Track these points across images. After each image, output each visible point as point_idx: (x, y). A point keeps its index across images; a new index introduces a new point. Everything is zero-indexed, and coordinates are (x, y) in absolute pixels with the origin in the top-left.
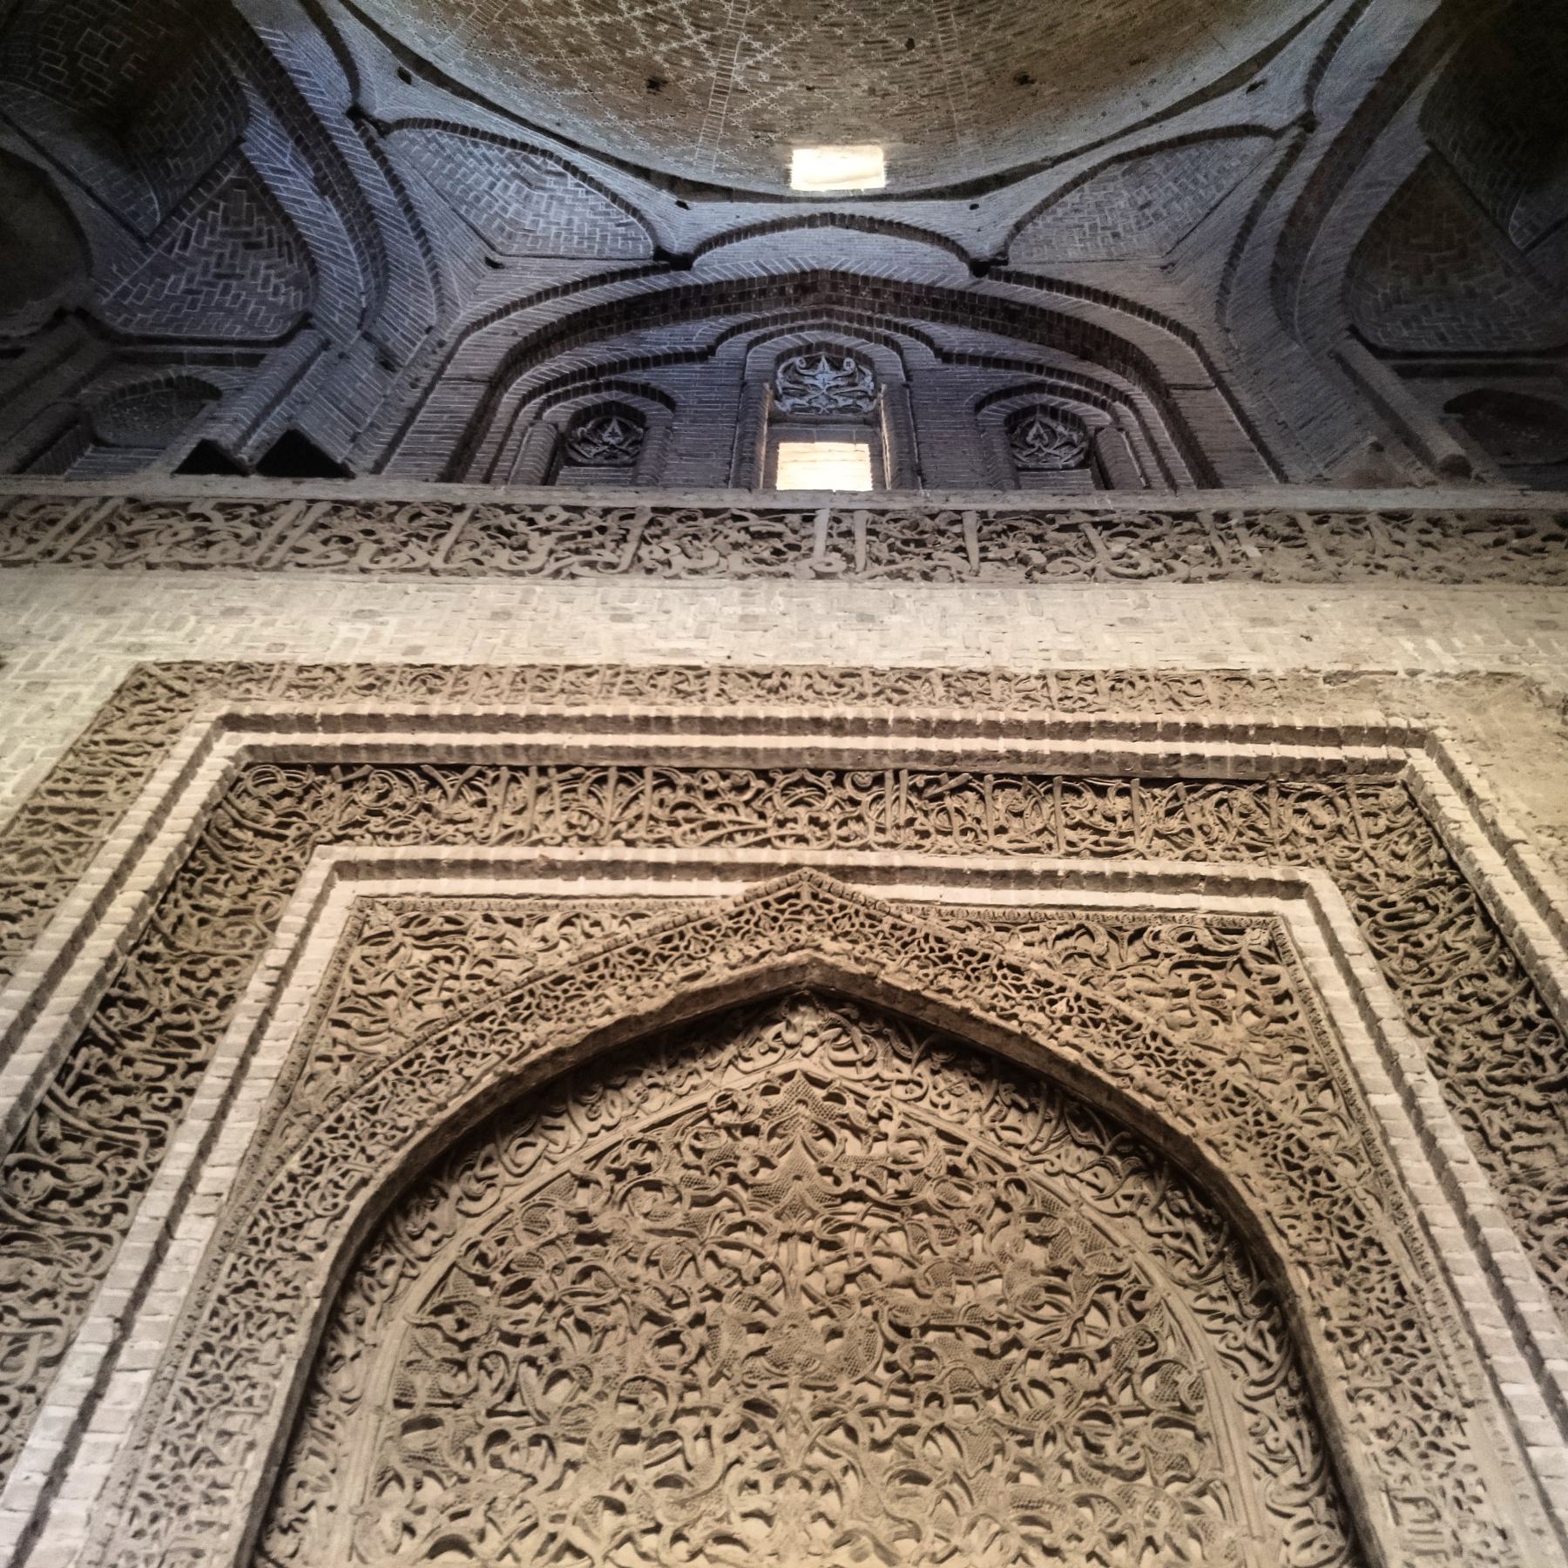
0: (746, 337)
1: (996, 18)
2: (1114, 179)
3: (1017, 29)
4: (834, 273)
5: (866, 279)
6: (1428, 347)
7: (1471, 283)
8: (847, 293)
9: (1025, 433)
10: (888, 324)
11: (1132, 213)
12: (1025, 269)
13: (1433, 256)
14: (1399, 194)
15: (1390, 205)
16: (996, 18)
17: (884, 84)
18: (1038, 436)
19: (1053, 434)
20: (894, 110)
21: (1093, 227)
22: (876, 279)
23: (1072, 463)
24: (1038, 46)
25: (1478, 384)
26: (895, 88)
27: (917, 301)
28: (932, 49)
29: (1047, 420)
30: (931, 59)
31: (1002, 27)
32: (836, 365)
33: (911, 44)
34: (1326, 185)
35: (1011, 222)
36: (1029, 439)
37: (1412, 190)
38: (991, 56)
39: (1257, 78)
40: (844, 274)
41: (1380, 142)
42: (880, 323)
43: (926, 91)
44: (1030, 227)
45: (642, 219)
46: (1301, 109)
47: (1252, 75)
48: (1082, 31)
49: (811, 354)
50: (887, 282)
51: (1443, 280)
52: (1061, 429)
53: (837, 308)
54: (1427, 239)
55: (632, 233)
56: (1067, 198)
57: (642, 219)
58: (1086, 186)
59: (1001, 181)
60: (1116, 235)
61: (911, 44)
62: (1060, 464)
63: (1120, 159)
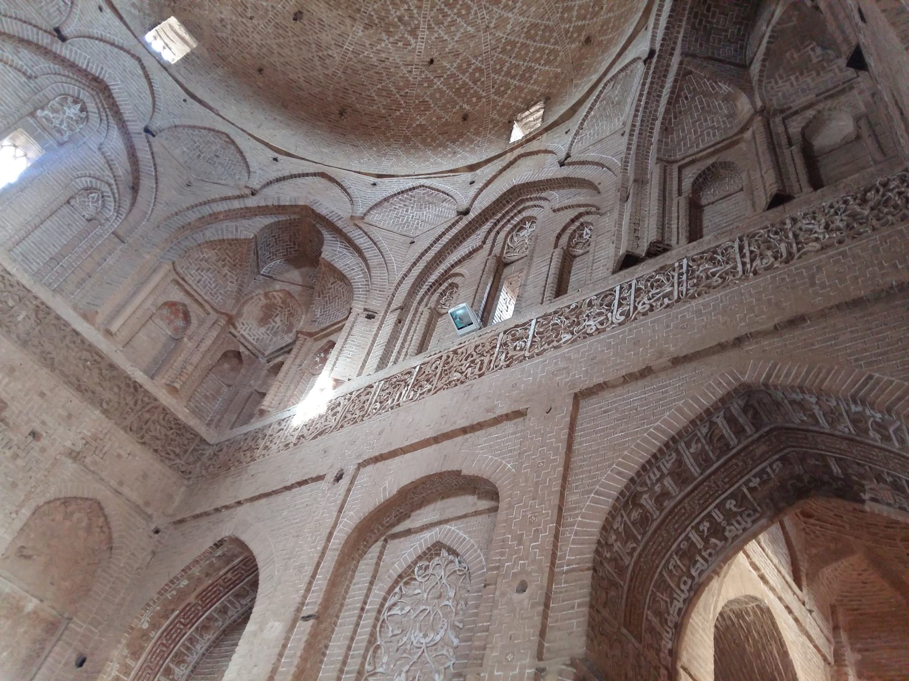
0: (59, 78)
1: (282, 40)
2: (221, 139)
3: (281, 52)
4: (107, 86)
5: (113, 98)
6: (190, 282)
7: (229, 274)
8: (107, 94)
9: (91, 193)
10: (107, 116)
11: (212, 155)
12: (153, 144)
13: (228, 259)
14: (233, 240)
15: (228, 240)
16: (282, 40)
17: (229, 22)
18: (93, 198)
19: (98, 200)
20: (219, 34)
21: (198, 147)
22: (115, 102)
23: (87, 216)
24: (278, 64)
25: (187, 301)
26: (229, 27)
27: (120, 120)
28: (255, 27)
29: (100, 196)
30: (251, 30)
31: (279, 45)
32: (82, 110)
33: (251, 18)
34: (231, 215)
35: (177, 122)
36: (91, 195)
37: (235, 243)
38: (264, 50)
39: (280, 157)
40: (109, 90)
41: (258, 218)
42: (106, 112)
43: (235, 38)
44: (181, 129)
45: (71, 7)
46: (258, 187)
47: (282, 154)
48: (291, 76)
49: (76, 101)
50: (117, 106)
51: (224, 266)
52: (100, 202)
53: (100, 95)
54: (231, 254)
55: (63, 9)
56: (202, 130)
57: (71, 7)
58: (212, 133)
59: (200, 102)
60: (199, 156)
61: (251, 18)
62: (84, 213)
63: (228, 136)
